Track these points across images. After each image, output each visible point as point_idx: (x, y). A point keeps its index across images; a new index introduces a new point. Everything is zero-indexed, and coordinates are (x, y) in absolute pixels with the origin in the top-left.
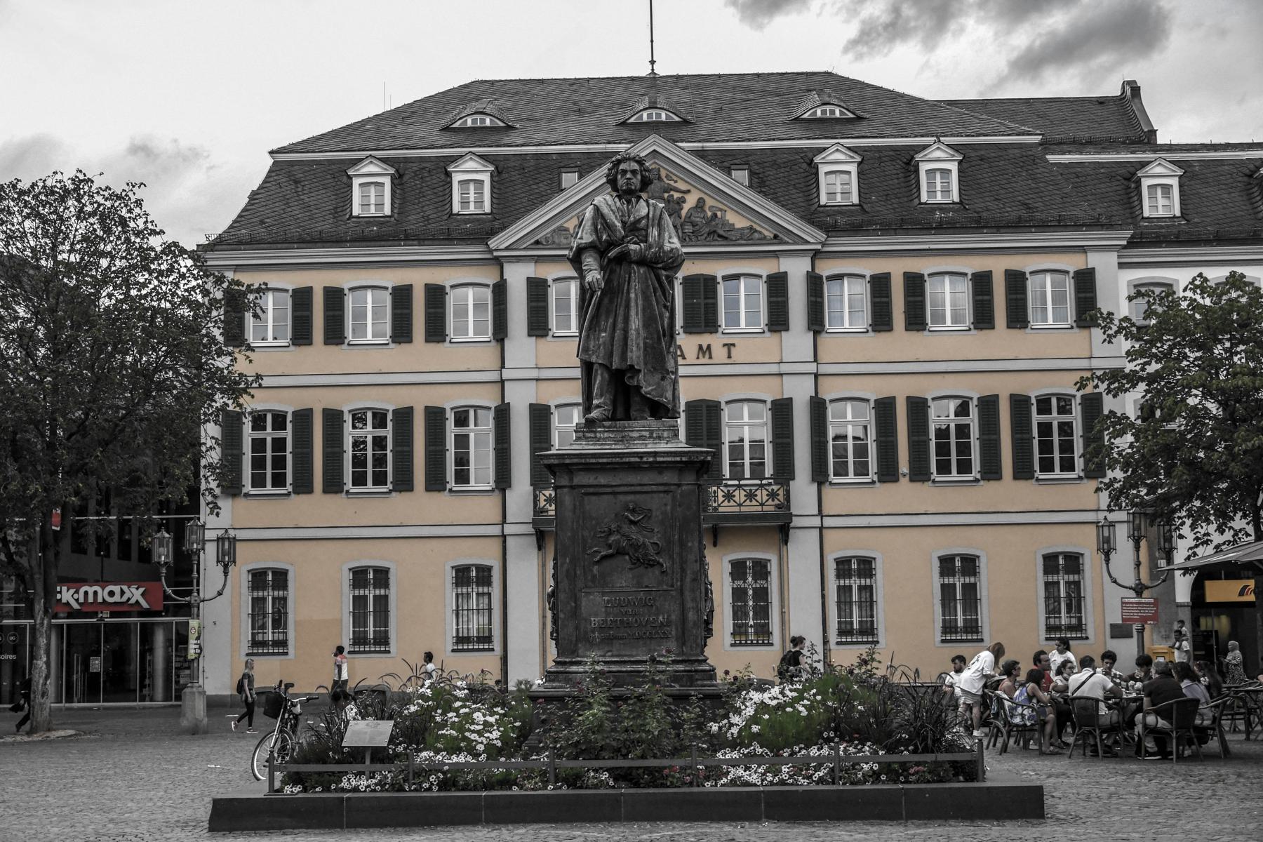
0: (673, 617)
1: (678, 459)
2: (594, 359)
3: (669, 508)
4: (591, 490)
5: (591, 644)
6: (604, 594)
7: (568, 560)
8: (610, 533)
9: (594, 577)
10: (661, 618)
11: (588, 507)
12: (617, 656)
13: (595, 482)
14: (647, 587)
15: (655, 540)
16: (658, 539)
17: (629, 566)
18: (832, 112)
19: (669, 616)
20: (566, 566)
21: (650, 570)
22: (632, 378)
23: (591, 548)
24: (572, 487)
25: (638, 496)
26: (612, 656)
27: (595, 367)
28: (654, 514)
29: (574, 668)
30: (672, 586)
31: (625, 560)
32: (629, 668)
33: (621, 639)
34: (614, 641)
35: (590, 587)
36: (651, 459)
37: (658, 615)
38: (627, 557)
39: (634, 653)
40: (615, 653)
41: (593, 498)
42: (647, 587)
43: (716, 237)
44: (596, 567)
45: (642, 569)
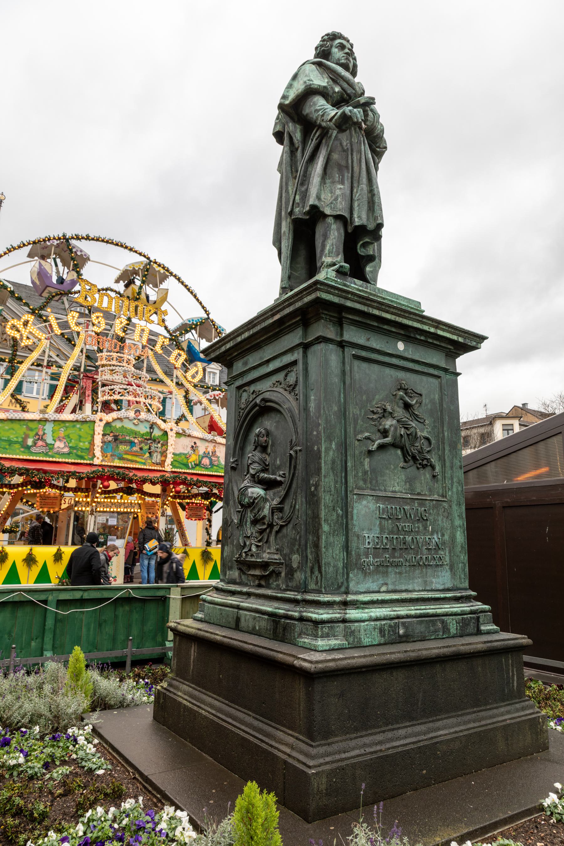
0: (446, 537)
1: (455, 338)
2: (328, 211)
3: (437, 397)
4: (364, 354)
5: (365, 572)
6: (378, 498)
7: (333, 446)
8: (385, 413)
9: (365, 473)
10: (435, 537)
11: (357, 376)
12: (395, 591)
13: (368, 344)
14: (419, 494)
15: (425, 434)
16: (429, 433)
17: (402, 464)
18: (84, 310)
19: (443, 535)
20: (331, 453)
21: (422, 471)
22: (365, 245)
23: (362, 432)
24: (342, 345)
25: (408, 375)
26: (388, 592)
27: (330, 220)
28: (424, 401)
29: (353, 614)
30: (443, 496)
31: (397, 454)
32: (412, 610)
33: (397, 566)
34: (390, 569)
35: (363, 489)
36: (432, 330)
37: (432, 534)
38: (399, 452)
39: (410, 587)
40: (391, 587)
41: (365, 365)
42: (419, 494)
43: (27, 349)
44: (367, 460)
45: (412, 470)
